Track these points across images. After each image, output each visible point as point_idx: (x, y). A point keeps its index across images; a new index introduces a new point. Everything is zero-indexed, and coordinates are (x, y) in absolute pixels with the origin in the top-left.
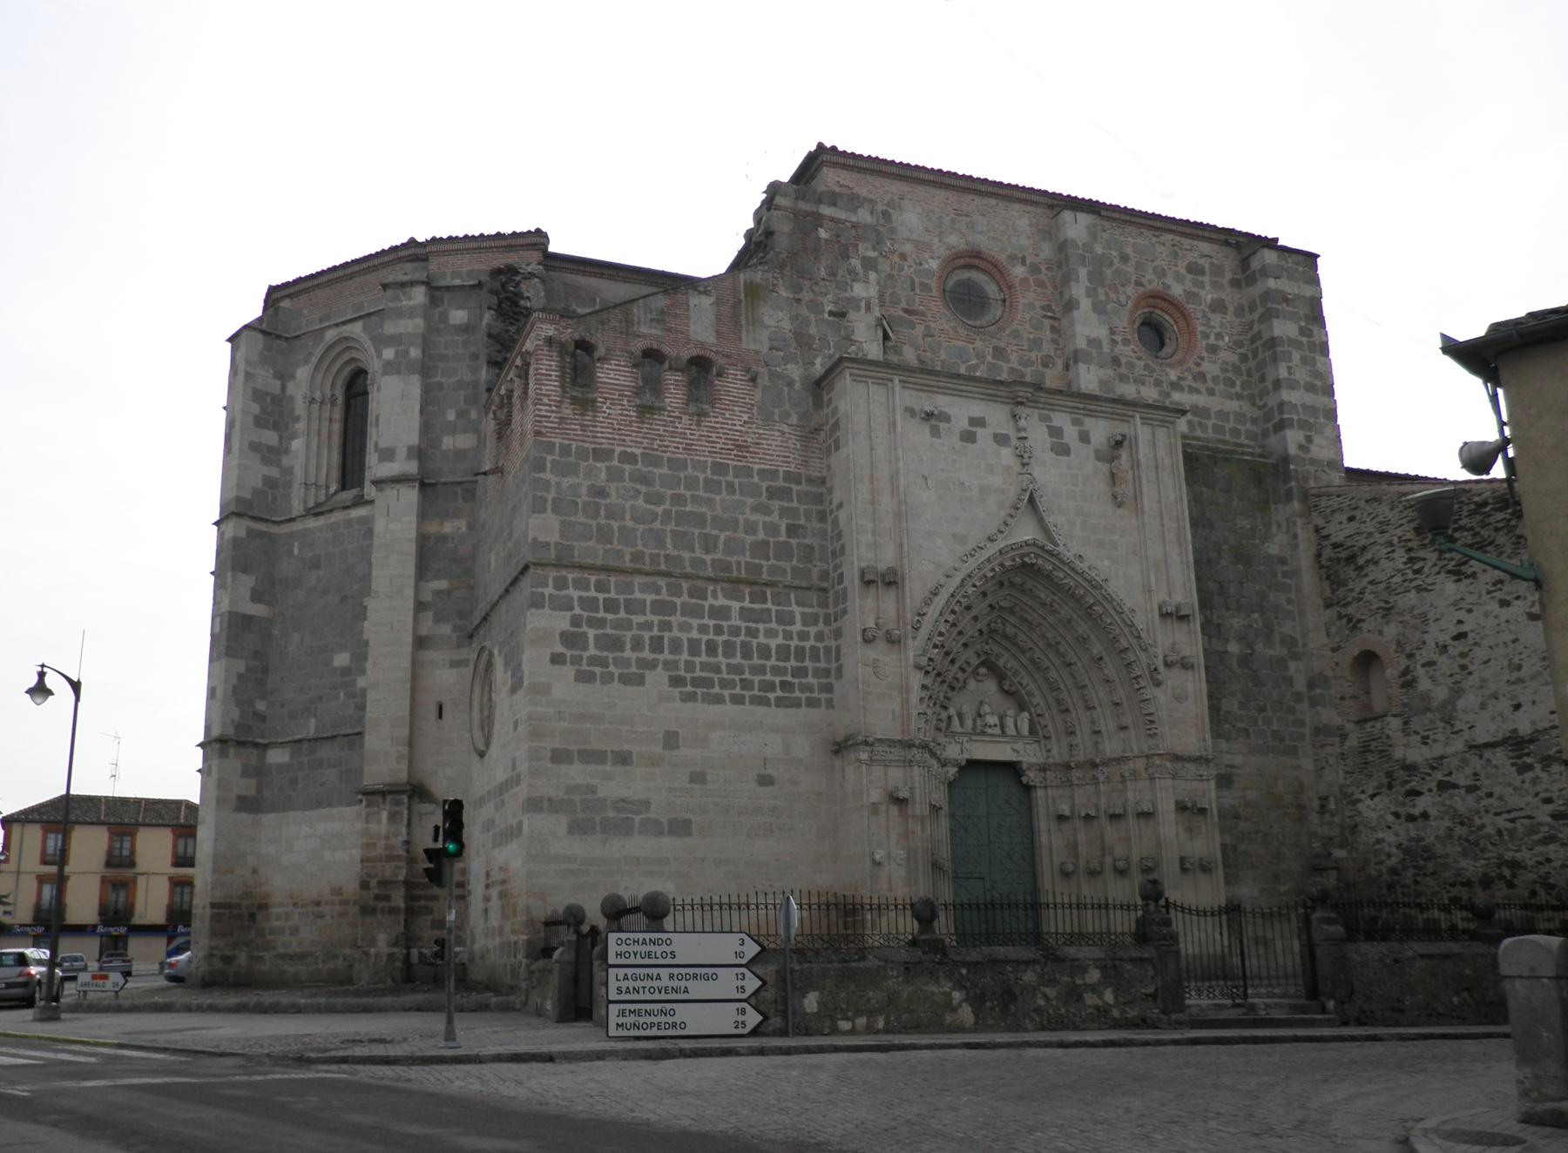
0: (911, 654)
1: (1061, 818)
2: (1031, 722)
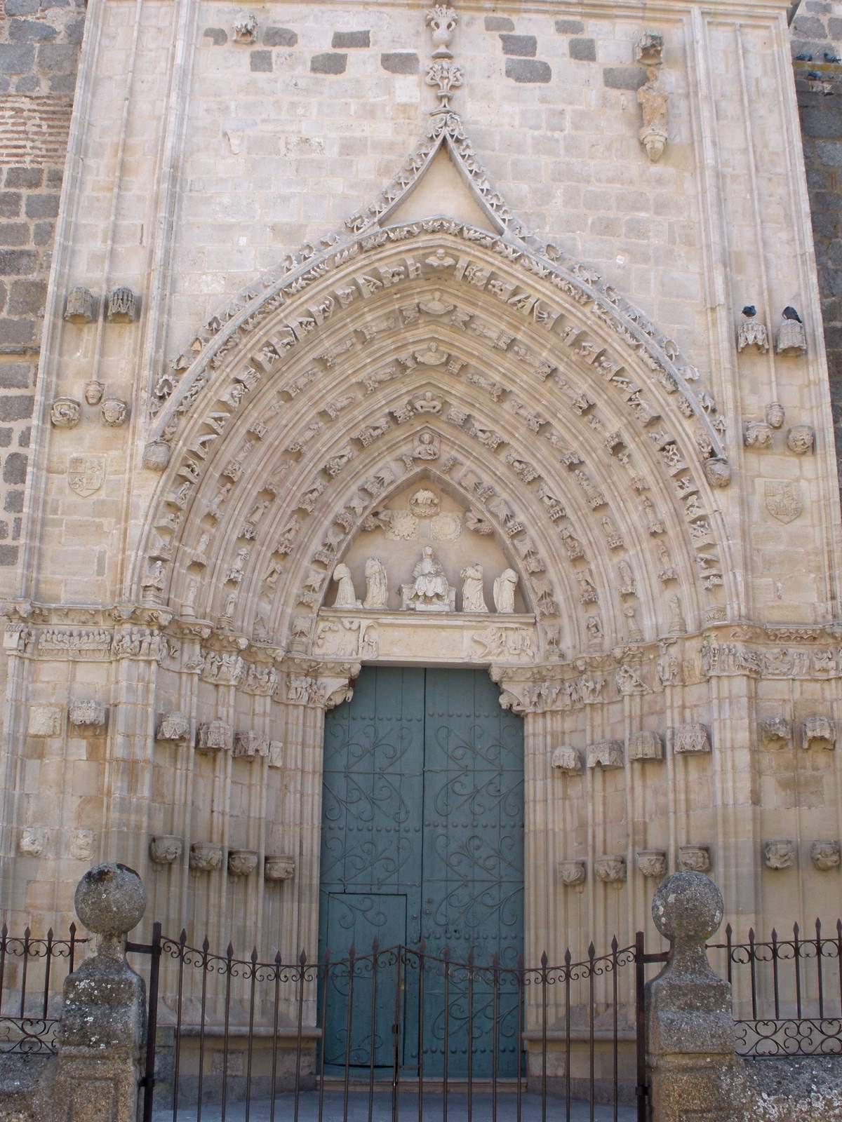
0: (141, 445)
2: (519, 589)
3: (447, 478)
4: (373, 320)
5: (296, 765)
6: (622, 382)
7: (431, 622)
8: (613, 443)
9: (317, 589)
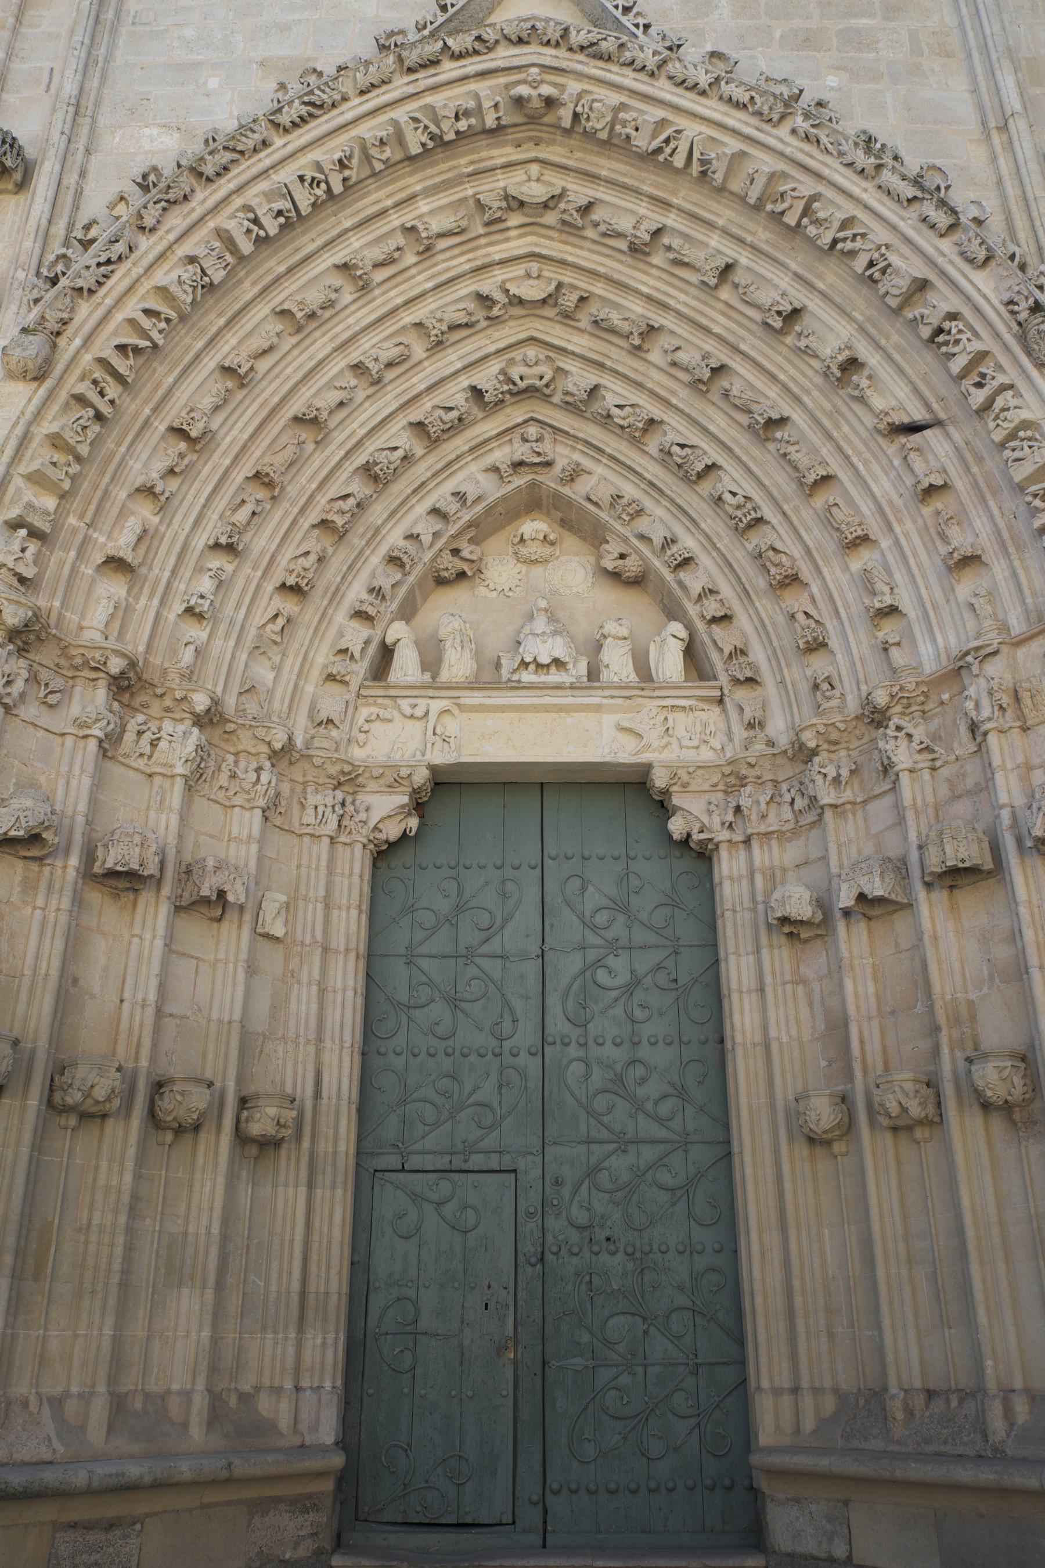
1: (790, 928)
2: (691, 652)
3: (566, 491)
4: (432, 212)
5: (313, 936)
6: (854, 238)
7: (547, 700)
8: (841, 358)
9: (357, 655)
